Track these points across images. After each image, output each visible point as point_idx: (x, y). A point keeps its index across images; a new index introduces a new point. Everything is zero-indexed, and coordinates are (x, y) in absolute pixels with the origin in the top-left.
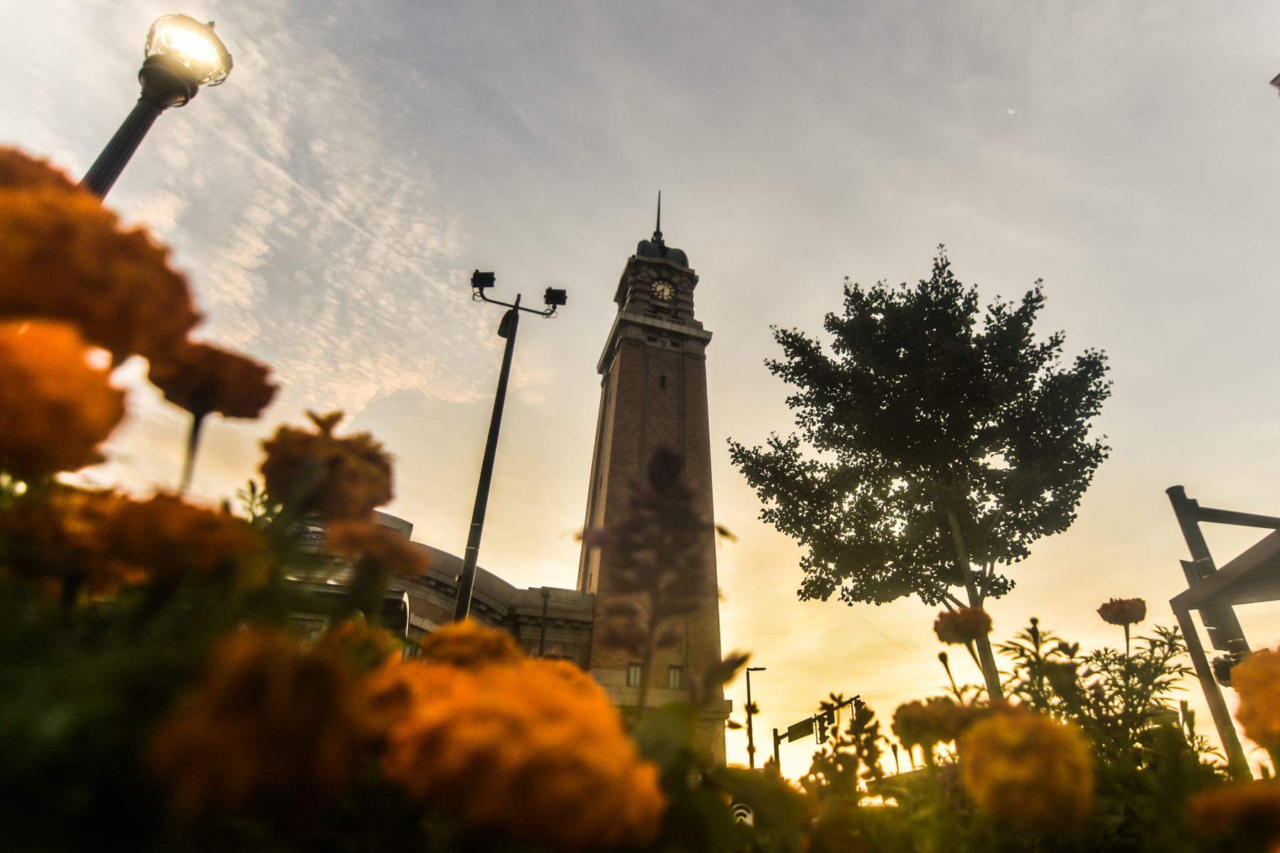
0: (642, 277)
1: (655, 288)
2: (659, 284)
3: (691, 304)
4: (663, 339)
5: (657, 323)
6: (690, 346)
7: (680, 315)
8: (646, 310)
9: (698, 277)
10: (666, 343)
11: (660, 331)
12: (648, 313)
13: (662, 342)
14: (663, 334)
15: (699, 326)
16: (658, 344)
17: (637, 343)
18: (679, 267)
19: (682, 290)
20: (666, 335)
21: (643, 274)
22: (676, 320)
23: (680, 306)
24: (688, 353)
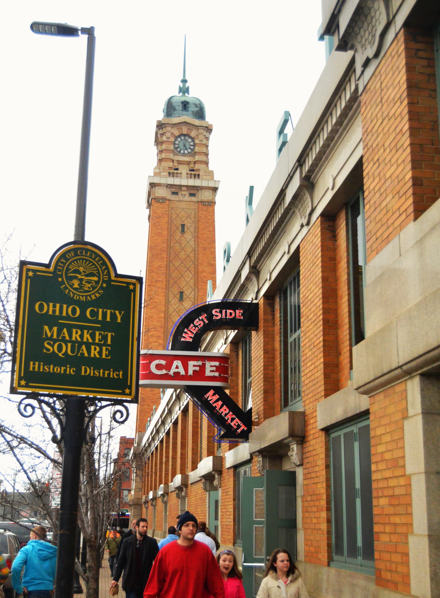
0: (167, 138)
3: (207, 155)
4: (183, 193)
5: (177, 181)
6: (205, 196)
7: (197, 166)
8: (170, 168)
9: (211, 125)
11: (180, 186)
14: (183, 189)
15: (211, 174)
16: (179, 197)
17: (163, 200)
18: (197, 122)
21: (168, 134)
22: (193, 173)
23: (197, 158)
24: (201, 202)
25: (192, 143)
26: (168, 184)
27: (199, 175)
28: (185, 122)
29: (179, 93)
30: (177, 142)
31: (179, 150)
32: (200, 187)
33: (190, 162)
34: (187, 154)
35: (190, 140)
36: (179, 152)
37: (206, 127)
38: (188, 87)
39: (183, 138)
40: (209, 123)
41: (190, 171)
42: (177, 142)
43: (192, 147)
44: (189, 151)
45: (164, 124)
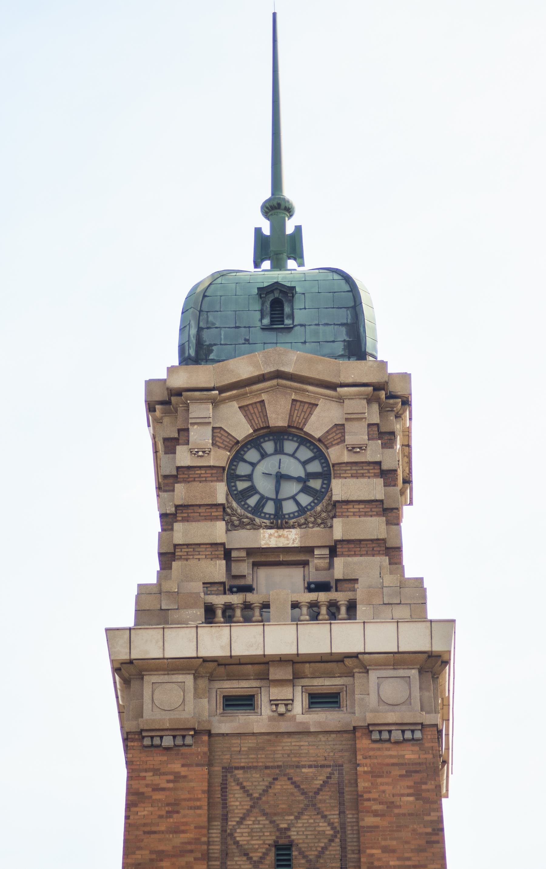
1: (249, 477)
2: (264, 455)
4: (277, 693)
8: (208, 585)
10: (289, 703)
12: (219, 600)
13: (275, 703)
14: (275, 673)
19: (346, 457)
20: (286, 673)
22: (322, 597)
24: (368, 729)
25: (315, 467)
26: (205, 660)
27: (352, 607)
28: (279, 375)
29: (257, 265)
30: (243, 469)
31: (252, 501)
32: (355, 656)
33: (309, 550)
34: (293, 515)
35: (305, 453)
36: (258, 510)
37: (378, 387)
38: (298, 229)
39: (269, 447)
40: (391, 369)
41: (309, 589)
42: (243, 469)
43: (316, 484)
44: (305, 500)
45: (178, 393)
